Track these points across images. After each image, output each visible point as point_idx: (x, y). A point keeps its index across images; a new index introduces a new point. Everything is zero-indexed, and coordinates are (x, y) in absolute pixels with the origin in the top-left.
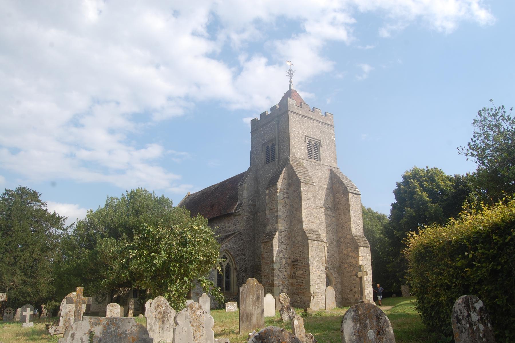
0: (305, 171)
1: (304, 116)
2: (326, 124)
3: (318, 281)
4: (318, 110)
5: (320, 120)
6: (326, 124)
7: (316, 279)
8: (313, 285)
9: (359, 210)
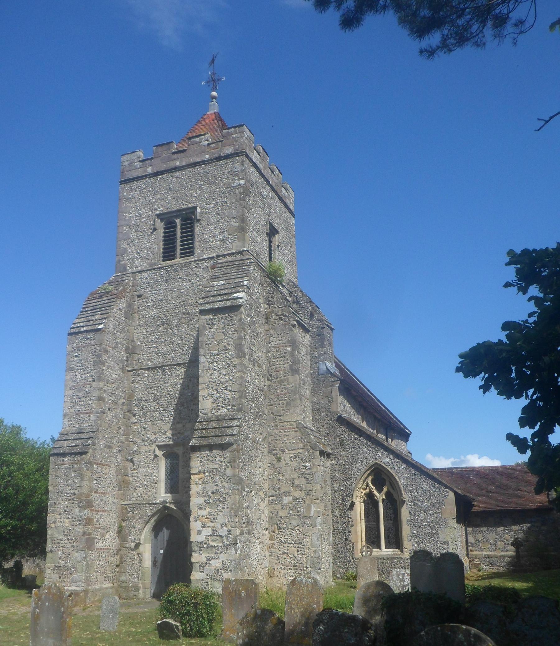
0: (107, 301)
1: (155, 175)
2: (219, 159)
3: (66, 542)
4: (197, 139)
5: (203, 159)
6: (219, 159)
7: (61, 537)
8: (51, 551)
9: (232, 348)
